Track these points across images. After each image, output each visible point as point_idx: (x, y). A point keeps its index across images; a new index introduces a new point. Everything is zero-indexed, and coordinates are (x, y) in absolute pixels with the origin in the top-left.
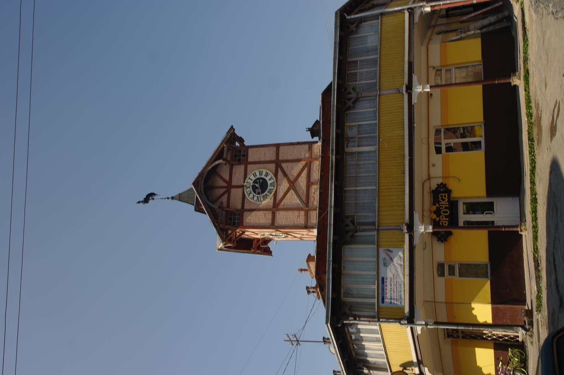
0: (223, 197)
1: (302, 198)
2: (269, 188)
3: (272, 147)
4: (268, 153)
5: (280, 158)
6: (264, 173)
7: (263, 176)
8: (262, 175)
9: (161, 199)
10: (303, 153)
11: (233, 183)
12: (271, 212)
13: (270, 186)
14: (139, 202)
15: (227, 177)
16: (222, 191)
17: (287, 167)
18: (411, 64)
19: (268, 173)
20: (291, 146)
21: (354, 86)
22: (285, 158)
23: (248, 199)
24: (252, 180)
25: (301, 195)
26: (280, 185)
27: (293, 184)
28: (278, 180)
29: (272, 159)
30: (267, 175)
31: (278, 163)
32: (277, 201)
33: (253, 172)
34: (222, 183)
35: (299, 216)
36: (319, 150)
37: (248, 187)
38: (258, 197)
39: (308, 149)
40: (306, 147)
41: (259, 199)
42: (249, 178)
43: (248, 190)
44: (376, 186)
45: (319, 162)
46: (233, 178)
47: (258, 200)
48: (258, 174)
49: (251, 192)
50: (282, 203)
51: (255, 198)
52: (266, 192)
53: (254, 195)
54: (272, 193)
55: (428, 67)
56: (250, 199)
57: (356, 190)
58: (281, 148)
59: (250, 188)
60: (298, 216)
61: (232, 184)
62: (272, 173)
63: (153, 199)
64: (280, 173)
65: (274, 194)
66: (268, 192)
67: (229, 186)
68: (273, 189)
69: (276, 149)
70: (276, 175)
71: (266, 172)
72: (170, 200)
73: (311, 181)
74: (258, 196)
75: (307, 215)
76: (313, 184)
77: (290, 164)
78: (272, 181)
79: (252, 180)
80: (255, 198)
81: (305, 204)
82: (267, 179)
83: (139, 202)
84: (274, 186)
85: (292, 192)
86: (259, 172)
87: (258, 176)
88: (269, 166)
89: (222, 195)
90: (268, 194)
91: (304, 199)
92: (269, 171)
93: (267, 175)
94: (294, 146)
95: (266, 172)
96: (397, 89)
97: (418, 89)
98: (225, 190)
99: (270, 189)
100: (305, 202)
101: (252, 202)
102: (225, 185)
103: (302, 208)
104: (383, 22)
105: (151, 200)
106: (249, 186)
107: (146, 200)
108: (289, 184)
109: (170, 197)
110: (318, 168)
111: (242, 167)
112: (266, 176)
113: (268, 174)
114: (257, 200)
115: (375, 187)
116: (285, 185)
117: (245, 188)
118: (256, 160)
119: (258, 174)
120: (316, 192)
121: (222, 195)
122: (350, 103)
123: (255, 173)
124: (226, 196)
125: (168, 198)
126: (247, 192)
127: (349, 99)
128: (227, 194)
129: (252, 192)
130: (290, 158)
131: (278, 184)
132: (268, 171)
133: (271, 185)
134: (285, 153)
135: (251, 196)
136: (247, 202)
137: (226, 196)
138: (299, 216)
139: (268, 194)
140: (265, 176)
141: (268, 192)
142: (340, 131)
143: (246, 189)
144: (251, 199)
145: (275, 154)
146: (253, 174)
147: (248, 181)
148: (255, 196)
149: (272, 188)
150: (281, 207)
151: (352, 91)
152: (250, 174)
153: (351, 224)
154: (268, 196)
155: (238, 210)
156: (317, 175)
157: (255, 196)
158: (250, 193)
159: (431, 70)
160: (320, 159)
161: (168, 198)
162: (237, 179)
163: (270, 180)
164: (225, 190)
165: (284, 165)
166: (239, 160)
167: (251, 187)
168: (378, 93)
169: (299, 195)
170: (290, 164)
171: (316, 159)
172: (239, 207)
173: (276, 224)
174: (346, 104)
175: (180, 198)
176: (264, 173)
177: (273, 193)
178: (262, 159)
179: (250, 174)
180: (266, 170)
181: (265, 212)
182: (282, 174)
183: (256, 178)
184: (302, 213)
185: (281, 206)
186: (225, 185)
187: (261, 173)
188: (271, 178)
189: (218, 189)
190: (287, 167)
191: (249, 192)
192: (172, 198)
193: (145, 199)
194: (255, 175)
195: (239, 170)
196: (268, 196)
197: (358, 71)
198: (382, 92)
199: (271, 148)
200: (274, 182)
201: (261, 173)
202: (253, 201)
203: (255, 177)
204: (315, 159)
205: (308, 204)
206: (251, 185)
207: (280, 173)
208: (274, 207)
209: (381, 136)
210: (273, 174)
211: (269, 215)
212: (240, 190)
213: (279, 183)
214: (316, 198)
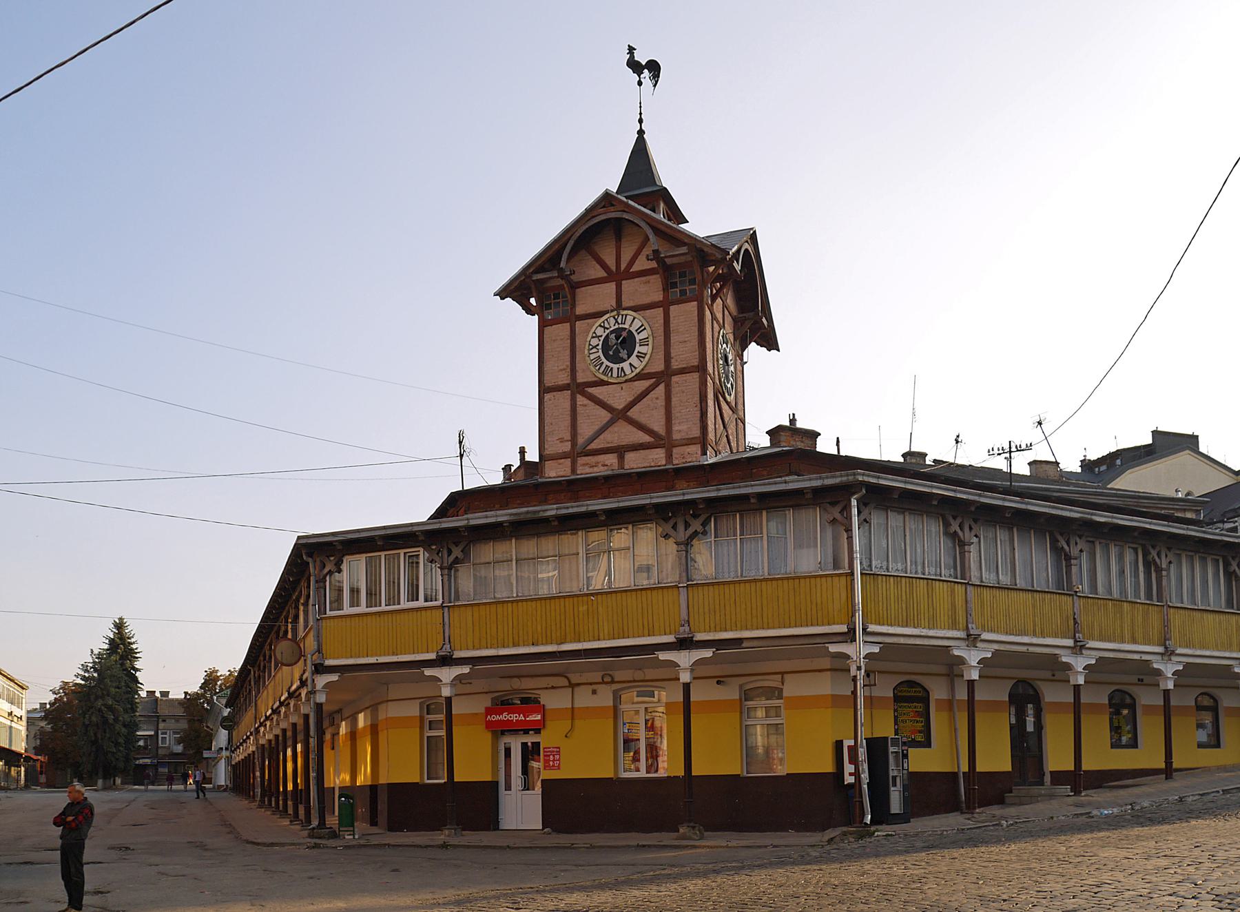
0: (598, 267)
1: (595, 441)
2: (615, 366)
3: (698, 357)
4: (687, 348)
5: (674, 379)
6: (643, 349)
7: (638, 348)
8: (640, 345)
9: (640, 103)
10: (684, 427)
11: (626, 284)
12: (568, 382)
13: (618, 369)
14: (631, 50)
15: (642, 264)
16: (611, 263)
17: (657, 398)
18: (737, 642)
19: (644, 358)
20: (698, 399)
21: (709, 534)
22: (675, 390)
23: (593, 325)
24: (630, 326)
25: (601, 437)
26: (622, 389)
27: (620, 415)
28: (630, 383)
29: (673, 361)
30: (641, 356)
31: (664, 377)
32: (590, 390)
33: (646, 325)
34: (626, 257)
35: (562, 440)
36: (690, 460)
37: (616, 320)
38: (595, 347)
39: (691, 436)
40: (696, 432)
41: (594, 350)
42: (634, 319)
43: (612, 321)
44: (517, 596)
45: (665, 465)
46: (636, 280)
47: (592, 349)
48: (643, 335)
49: (608, 329)
50: (586, 401)
51: (594, 342)
52: (606, 363)
53: (601, 336)
54: (605, 375)
55: (783, 673)
56: (593, 330)
57: (511, 561)
58: (696, 375)
59: (614, 325)
60: (563, 438)
61: (624, 282)
62: (645, 366)
63: (640, 83)
64: (646, 384)
65: (603, 380)
66: (607, 366)
67: (617, 276)
68: (612, 375)
69: (693, 366)
70: (640, 377)
71: (646, 354)
72: (639, 129)
73: (626, 453)
74: (600, 347)
75: (564, 456)
76: (621, 458)
77: (664, 404)
78: (628, 370)
79: (630, 326)
80: (594, 342)
81: (584, 448)
82: (633, 359)
83: (631, 50)
84: (618, 377)
85: (605, 416)
86: (647, 338)
87: (638, 337)
88: (661, 355)
89: (604, 266)
90: (604, 366)
91: (593, 446)
92: (649, 360)
93: (641, 356)
94: (699, 405)
95: (646, 354)
96: (688, 621)
97: (685, 659)
98: (614, 268)
99: (612, 368)
100: (587, 448)
101: (587, 335)
102: (623, 267)
103: (577, 445)
104: (836, 579)
105: (638, 79)
106: (620, 322)
107: (635, 66)
108: (622, 410)
109: (643, 128)
110: (652, 464)
111: (658, 296)
112: (637, 356)
113: (642, 359)
114: (591, 347)
115: (515, 595)
116: (618, 397)
117: (615, 313)
118: (671, 325)
119: (643, 335)
120: (606, 468)
121: (604, 266)
122: (668, 528)
123: (645, 329)
124: (602, 274)
125: (641, 121)
126: (607, 320)
127: (674, 527)
128: (606, 275)
129: (607, 331)
130: (674, 400)
131: (622, 385)
132: (647, 357)
133: (620, 370)
134: (684, 387)
135: (600, 331)
136: (588, 324)
137: (602, 274)
138: (561, 442)
139: (604, 366)
140: (638, 352)
141: (607, 366)
142: (603, 519)
143: (614, 318)
144: (594, 333)
145: (684, 366)
146: (642, 325)
147: (628, 316)
148: (600, 340)
149: (615, 374)
150: (578, 400)
151: (690, 531)
152: (643, 317)
153: (452, 558)
154: (599, 369)
155: (574, 306)
156: (640, 465)
157: (600, 340)
158: (605, 328)
159: (780, 676)
160: (671, 466)
161: (641, 121)
162: (635, 291)
163: (630, 364)
164: (614, 268)
165: (662, 387)
166: (674, 285)
167: (617, 326)
168: (683, 583)
169: (601, 434)
170: (661, 402)
171: (669, 457)
172: (580, 310)
173: (547, 396)
174: (666, 520)
175: (640, 156)
176: (643, 349)
177: (605, 378)
178: (674, 338)
179: (642, 319)
180: (649, 352)
181: (569, 370)
182: (644, 389)
183: (635, 334)
184: (567, 447)
185: (581, 400)
186: (623, 267)
187: (644, 342)
188: (634, 367)
189: (615, 252)
190: (657, 398)
191: (607, 325)
192: (641, 132)
193: (638, 63)
194: (639, 331)
195: (651, 290)
196: (599, 369)
197: (738, 538)
198: (683, 592)
199: (697, 353)
200: (625, 375)
201: (644, 342)
202: (588, 339)
203: (636, 331)
204: (672, 455)
205: (584, 456)
206: (621, 326)
207: (646, 384)
208: (579, 385)
209: (599, 596)
210: (643, 369)
211: (564, 379)
212: (614, 304)
213: (624, 385)
214: (596, 469)
